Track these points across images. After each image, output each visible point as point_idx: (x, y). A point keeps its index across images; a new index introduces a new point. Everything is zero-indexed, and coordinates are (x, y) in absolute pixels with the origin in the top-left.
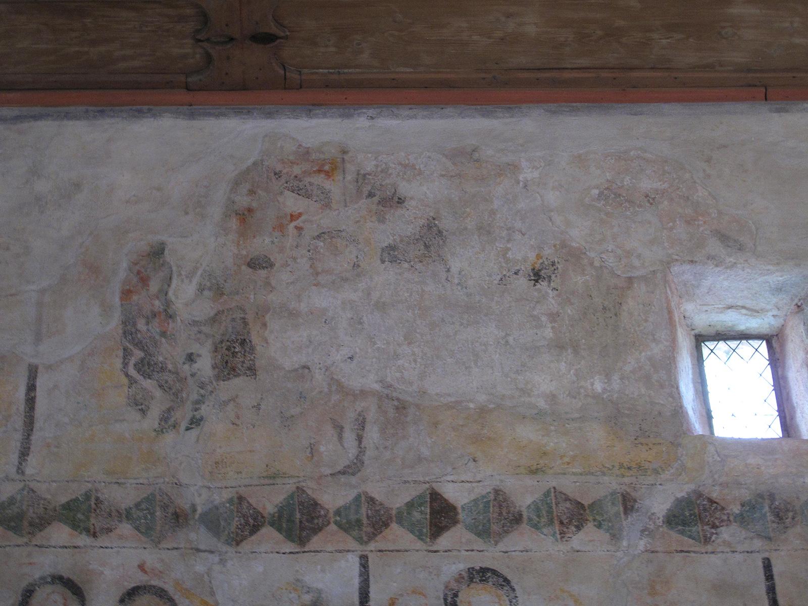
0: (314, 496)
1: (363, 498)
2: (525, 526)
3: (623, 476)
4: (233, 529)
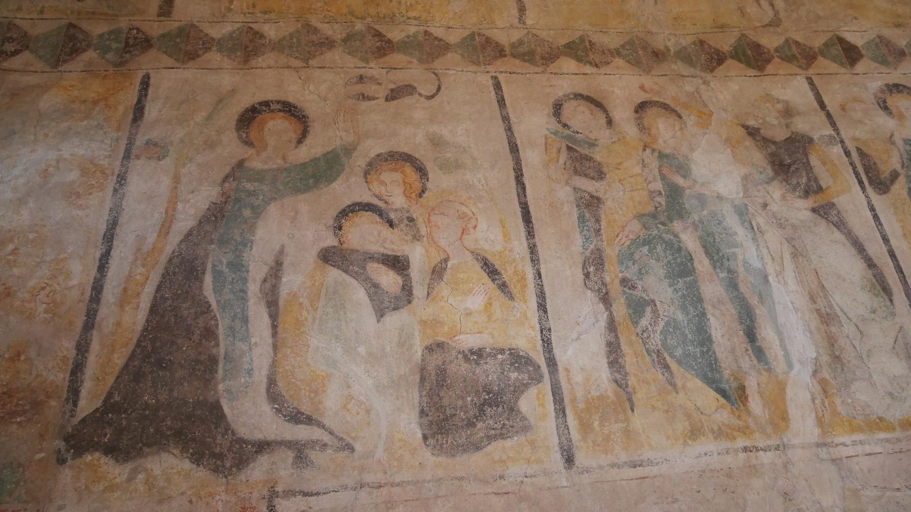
0: (755, 40)
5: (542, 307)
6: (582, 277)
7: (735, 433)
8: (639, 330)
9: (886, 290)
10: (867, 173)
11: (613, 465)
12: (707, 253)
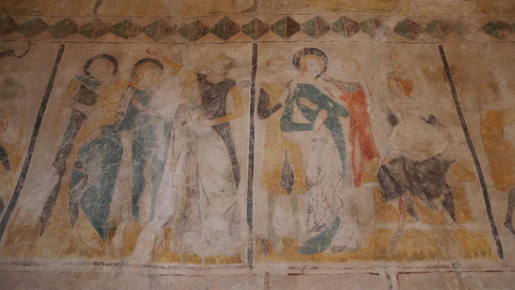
1: (256, 21)
2: (331, 31)
3: (375, 13)
4: (193, 34)
5: (24, 175)
6: (54, 159)
7: (93, 254)
8: (71, 192)
9: (237, 179)
10: (260, 104)
11: (13, 263)
12: (134, 150)
